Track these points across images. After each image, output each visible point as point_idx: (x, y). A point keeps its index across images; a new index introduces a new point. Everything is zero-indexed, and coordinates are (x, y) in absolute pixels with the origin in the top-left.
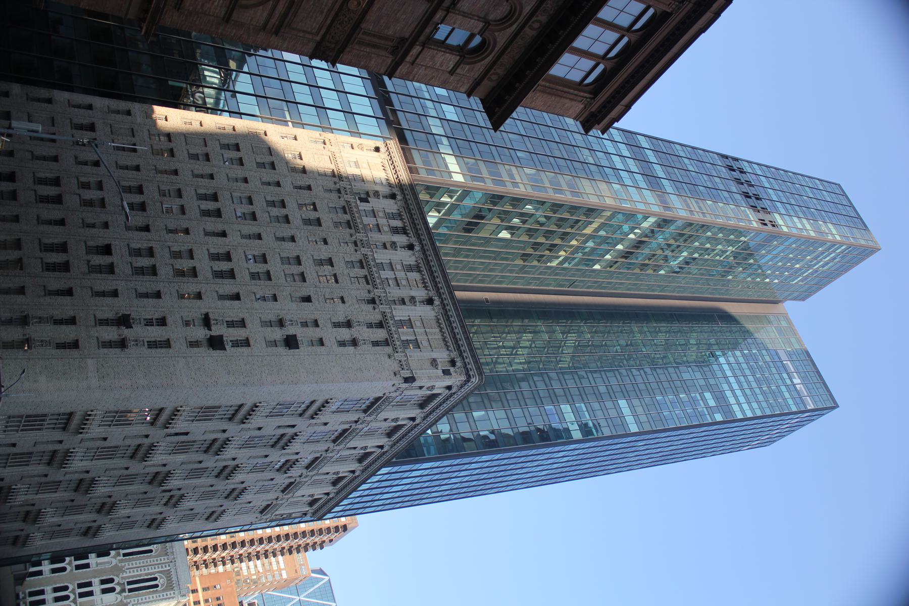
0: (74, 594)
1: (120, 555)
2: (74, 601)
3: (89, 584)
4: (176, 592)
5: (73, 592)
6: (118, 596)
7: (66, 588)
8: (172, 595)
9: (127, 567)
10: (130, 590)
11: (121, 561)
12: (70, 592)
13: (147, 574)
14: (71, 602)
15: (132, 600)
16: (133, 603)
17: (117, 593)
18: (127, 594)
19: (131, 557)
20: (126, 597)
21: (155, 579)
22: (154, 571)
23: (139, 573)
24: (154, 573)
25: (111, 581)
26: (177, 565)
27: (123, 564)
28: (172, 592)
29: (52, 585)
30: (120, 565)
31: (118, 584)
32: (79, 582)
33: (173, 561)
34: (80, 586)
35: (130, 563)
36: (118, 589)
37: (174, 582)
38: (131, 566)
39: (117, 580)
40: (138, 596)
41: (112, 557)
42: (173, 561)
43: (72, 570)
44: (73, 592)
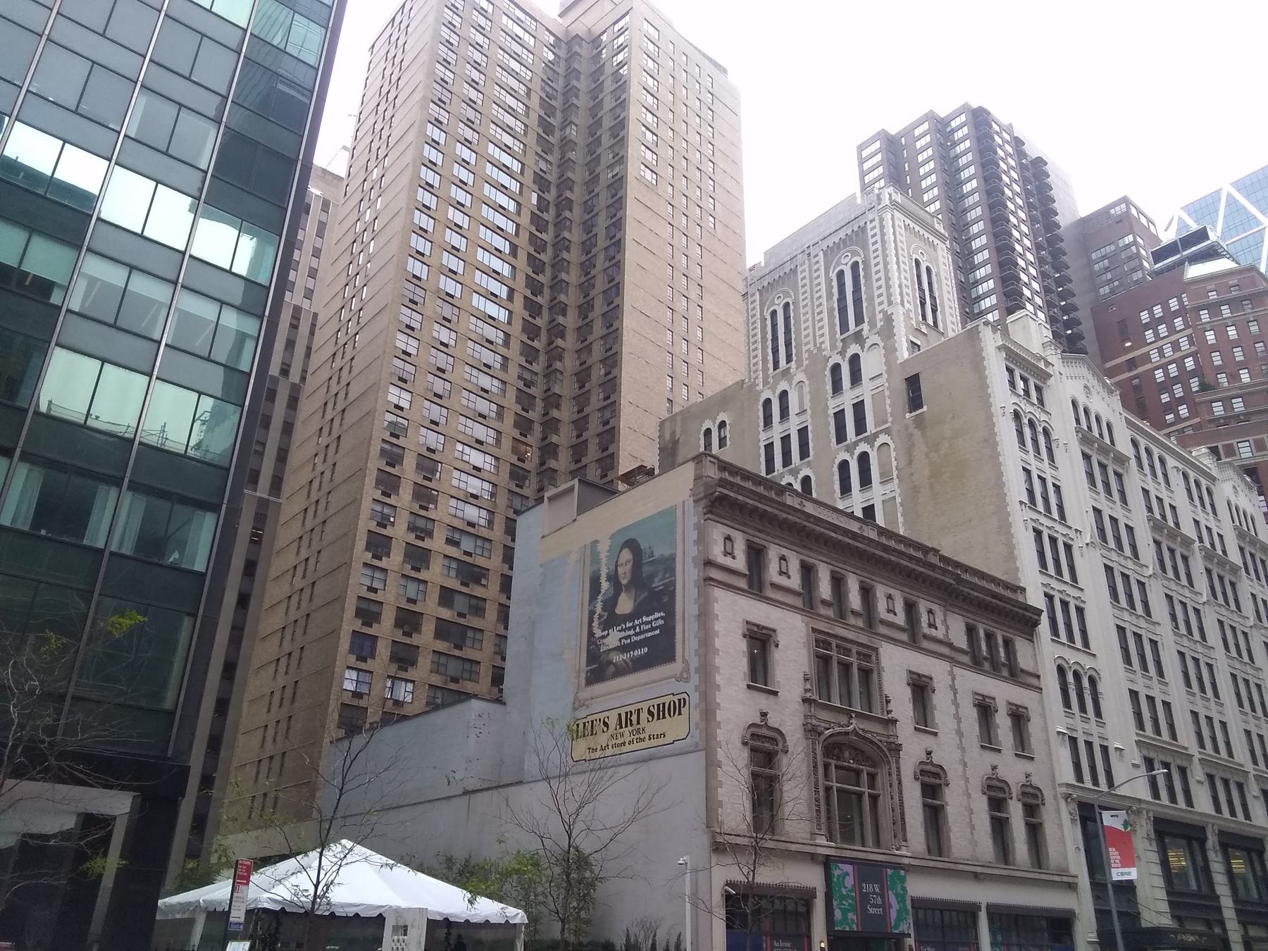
0: (856, 444)
2: (870, 440)
5: (850, 449)
7: (844, 466)
8: (876, 223)
9: (811, 346)
10: (860, 320)
11: (799, 364)
13: (830, 295)
15: (878, 309)
16: (885, 306)
18: (865, 327)
19: (794, 344)
21: (841, 275)
22: (823, 286)
24: (829, 281)
26: (816, 241)
27: (805, 355)
28: (869, 226)
30: (805, 363)
31: (842, 353)
32: (834, 440)
33: (807, 252)
34: (841, 437)
35: (804, 341)
36: (854, 349)
37: (849, 232)
38: (811, 338)
39: (836, 359)
40: (871, 299)
41: (790, 384)
43: (809, 465)
44: (850, 449)
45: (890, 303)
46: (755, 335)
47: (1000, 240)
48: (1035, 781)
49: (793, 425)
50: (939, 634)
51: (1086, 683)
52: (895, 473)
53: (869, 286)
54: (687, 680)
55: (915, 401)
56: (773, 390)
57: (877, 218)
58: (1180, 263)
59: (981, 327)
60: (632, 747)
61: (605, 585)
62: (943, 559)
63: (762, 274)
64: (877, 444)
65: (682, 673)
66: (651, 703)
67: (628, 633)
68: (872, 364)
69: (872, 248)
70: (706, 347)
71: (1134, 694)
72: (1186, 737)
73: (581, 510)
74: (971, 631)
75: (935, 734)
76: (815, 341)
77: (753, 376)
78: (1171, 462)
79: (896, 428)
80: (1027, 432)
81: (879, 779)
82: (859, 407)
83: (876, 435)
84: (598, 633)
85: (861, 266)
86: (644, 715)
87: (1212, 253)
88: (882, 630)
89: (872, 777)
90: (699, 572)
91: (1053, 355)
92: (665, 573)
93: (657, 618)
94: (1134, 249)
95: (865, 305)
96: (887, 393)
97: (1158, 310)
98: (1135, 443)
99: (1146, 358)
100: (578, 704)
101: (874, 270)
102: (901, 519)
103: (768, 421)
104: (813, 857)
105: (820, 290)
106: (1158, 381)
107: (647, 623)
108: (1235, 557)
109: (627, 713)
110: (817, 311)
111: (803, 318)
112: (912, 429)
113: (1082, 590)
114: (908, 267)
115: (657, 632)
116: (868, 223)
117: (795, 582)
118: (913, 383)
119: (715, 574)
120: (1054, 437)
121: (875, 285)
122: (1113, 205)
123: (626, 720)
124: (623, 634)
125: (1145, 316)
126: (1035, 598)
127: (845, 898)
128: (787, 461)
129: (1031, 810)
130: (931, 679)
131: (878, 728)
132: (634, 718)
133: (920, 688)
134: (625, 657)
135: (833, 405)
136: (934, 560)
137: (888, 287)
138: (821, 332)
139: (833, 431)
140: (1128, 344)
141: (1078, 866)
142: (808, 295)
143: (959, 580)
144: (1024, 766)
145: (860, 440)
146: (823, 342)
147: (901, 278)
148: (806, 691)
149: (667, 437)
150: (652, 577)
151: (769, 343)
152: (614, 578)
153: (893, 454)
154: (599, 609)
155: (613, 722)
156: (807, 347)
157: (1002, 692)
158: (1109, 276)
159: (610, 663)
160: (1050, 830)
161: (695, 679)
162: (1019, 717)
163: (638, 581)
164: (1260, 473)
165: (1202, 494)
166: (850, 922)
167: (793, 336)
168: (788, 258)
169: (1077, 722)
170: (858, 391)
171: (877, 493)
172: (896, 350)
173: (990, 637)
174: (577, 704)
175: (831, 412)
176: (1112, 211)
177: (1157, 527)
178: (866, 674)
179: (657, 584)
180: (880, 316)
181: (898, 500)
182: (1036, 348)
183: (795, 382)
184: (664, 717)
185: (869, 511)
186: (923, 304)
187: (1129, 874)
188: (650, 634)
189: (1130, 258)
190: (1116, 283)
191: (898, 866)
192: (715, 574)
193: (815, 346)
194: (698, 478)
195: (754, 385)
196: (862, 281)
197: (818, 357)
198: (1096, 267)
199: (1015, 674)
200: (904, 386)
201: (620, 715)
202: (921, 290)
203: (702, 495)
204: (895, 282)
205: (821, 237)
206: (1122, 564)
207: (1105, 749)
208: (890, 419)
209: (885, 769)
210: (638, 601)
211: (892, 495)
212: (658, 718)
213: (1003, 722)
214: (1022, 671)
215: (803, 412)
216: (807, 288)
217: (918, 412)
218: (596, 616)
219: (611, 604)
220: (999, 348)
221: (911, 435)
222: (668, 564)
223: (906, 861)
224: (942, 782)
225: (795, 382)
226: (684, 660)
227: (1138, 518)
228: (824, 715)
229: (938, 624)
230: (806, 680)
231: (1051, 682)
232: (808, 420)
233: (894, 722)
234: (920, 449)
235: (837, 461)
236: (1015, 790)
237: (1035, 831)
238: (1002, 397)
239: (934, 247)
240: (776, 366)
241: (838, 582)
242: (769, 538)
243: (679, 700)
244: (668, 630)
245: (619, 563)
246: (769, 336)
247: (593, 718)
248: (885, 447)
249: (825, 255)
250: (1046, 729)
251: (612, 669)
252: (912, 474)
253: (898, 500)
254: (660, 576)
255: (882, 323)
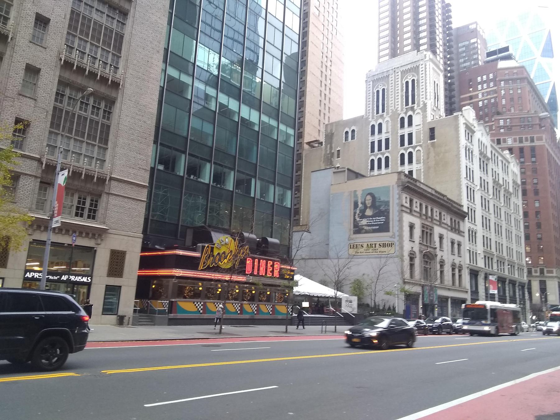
0: (408, 148)
1: (383, 115)
2: (414, 148)
3: (402, 137)
4: (421, 63)
5: (406, 149)
6: (416, 112)
7: (402, 155)
8: (423, 66)
9: (393, 108)
10: (413, 102)
11: (388, 114)
12: (406, 152)
13: (402, 90)
14: (414, 150)
15: (421, 100)
16: (424, 99)
17: (414, 113)
18: (416, 105)
19: (386, 106)
20: (418, 105)
21: (407, 83)
22: (400, 85)
23: (400, 97)
24: (402, 84)
25: (402, 119)
26: (398, 66)
27: (390, 111)
28: (421, 67)
29: (398, 167)
31: (406, 113)
32: (399, 145)
34: (402, 144)
35: (390, 105)
38: (393, 105)
39: (403, 115)
40: (419, 96)
41: (383, 121)
42: (394, 70)
43: (389, 152)
44: (406, 149)
45: (426, 99)
46: (370, 98)
47: (432, 42)
48: (462, 263)
49: (383, 137)
50: (445, 222)
51: (474, 234)
52: (422, 161)
53: (419, 90)
54: (394, 238)
55: (432, 137)
56: (376, 121)
57: (424, 64)
58: (497, 60)
59: (459, 116)
60: (372, 254)
61: (360, 205)
62: (448, 199)
63: (374, 74)
64: (417, 149)
65: (392, 236)
66: (381, 242)
67: (370, 221)
68: (417, 120)
69: (421, 76)
70: (332, 88)
71: (484, 236)
72: (493, 249)
73: (348, 179)
74: (451, 219)
75: (414, 242)
76: (395, 108)
77: (368, 114)
78: (500, 158)
79: (424, 145)
80: (467, 152)
81: (431, 263)
82: (410, 135)
83: (416, 146)
84: (358, 219)
85: (416, 82)
86: (377, 246)
87: (509, 57)
88: (435, 222)
89: (430, 263)
90: (399, 208)
91: (475, 123)
92: (385, 206)
93: (382, 219)
94: (476, 44)
95: (416, 97)
96: (422, 132)
97: (485, 77)
98: (492, 152)
99: (477, 96)
100: (350, 239)
101: (421, 84)
102: (422, 177)
103: (373, 133)
104: (420, 285)
105: (398, 87)
106: (480, 106)
107: (378, 219)
108: (511, 190)
109: (370, 244)
110: (396, 95)
111: (390, 96)
112: (430, 146)
113: (475, 205)
114: (432, 85)
115: (383, 223)
116: (420, 65)
117: (418, 210)
118: (432, 130)
119: (404, 209)
120: (473, 154)
121: (421, 90)
122: (471, 24)
123: (370, 246)
124: (368, 221)
125: (479, 79)
126: (465, 210)
127: (426, 295)
128: (380, 149)
129: (460, 271)
130: (443, 235)
131: (432, 250)
132: (374, 246)
133: (441, 237)
134: (369, 228)
135: (400, 132)
136: (445, 199)
137: (426, 93)
138: (398, 103)
139: (399, 142)
140: (471, 89)
141: (468, 286)
142: (393, 87)
143: (452, 205)
144: (460, 259)
145: (410, 147)
146: (398, 108)
147: (430, 89)
148: (420, 241)
149: (329, 131)
150: (380, 206)
151: (375, 103)
152: (364, 203)
153: (422, 154)
154: (358, 212)
155: (365, 246)
156: (391, 108)
157: (456, 237)
158: (464, 55)
159: (363, 229)
160: (463, 276)
161: (397, 238)
162: (459, 245)
163: (374, 205)
164: (513, 150)
165: (505, 169)
166: (427, 301)
167: (386, 103)
168: (386, 70)
169: (472, 247)
170: (410, 129)
171: (415, 167)
172: (427, 117)
173: (455, 221)
174: (350, 239)
175: (399, 135)
176: (470, 27)
177: (494, 182)
178: (431, 234)
179: (382, 208)
180: (422, 103)
181: (422, 170)
182: (471, 121)
183: (385, 120)
184: (385, 247)
185: (411, 172)
186: (435, 98)
187: (494, 292)
188: (379, 223)
189: (474, 48)
190: (467, 58)
191: (435, 287)
192: (404, 209)
193: (395, 108)
194: (399, 179)
195: (367, 118)
196: (416, 88)
197: (395, 113)
198: (460, 50)
199: (459, 232)
200: (428, 131)
201: (368, 244)
202: (435, 93)
203: (401, 184)
204: (428, 91)
205: (400, 65)
206: (485, 195)
207: (476, 253)
208: (422, 142)
209: (434, 262)
210: (375, 212)
211: (420, 168)
212: (383, 247)
213: (456, 246)
214: (461, 231)
215: (387, 132)
216: (393, 84)
217: (433, 141)
218: (357, 214)
219: (363, 211)
220: (464, 123)
221: (429, 149)
222: (387, 203)
223: (437, 285)
224: (414, 256)
225: (385, 120)
226: (393, 232)
227: (490, 180)
228: (423, 247)
229: (446, 219)
230: (420, 238)
231: (466, 235)
232: (389, 136)
233: (436, 248)
234: (432, 154)
235: (400, 153)
236: (457, 265)
237: (460, 276)
238: (463, 141)
239: (439, 75)
240: (378, 113)
241: (426, 207)
242: (414, 197)
243: (391, 243)
244: (387, 223)
245: (366, 199)
246: (375, 100)
247: (358, 243)
248: (418, 151)
249: (401, 73)
250: (464, 248)
251: (364, 231)
252: (428, 162)
253: (422, 170)
254: (383, 206)
255: (422, 106)
